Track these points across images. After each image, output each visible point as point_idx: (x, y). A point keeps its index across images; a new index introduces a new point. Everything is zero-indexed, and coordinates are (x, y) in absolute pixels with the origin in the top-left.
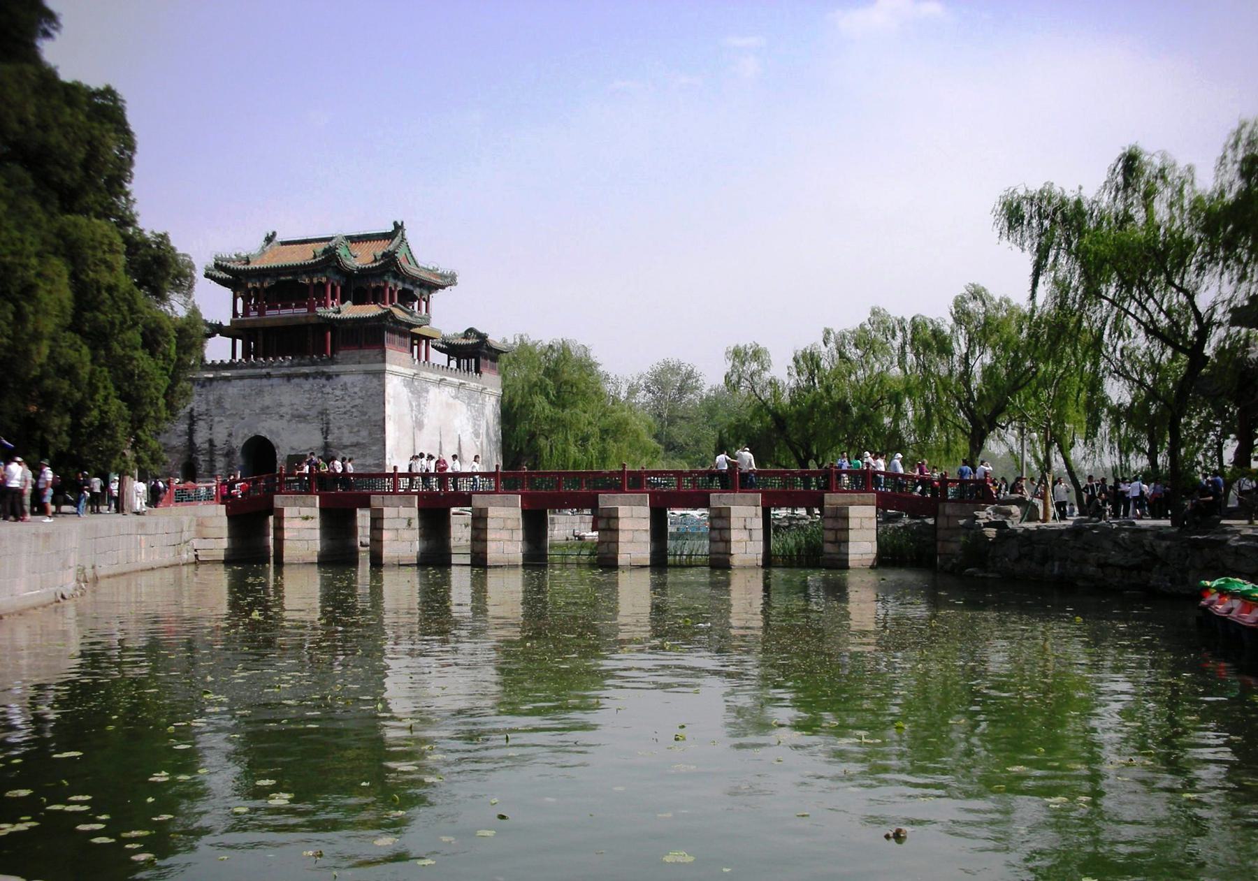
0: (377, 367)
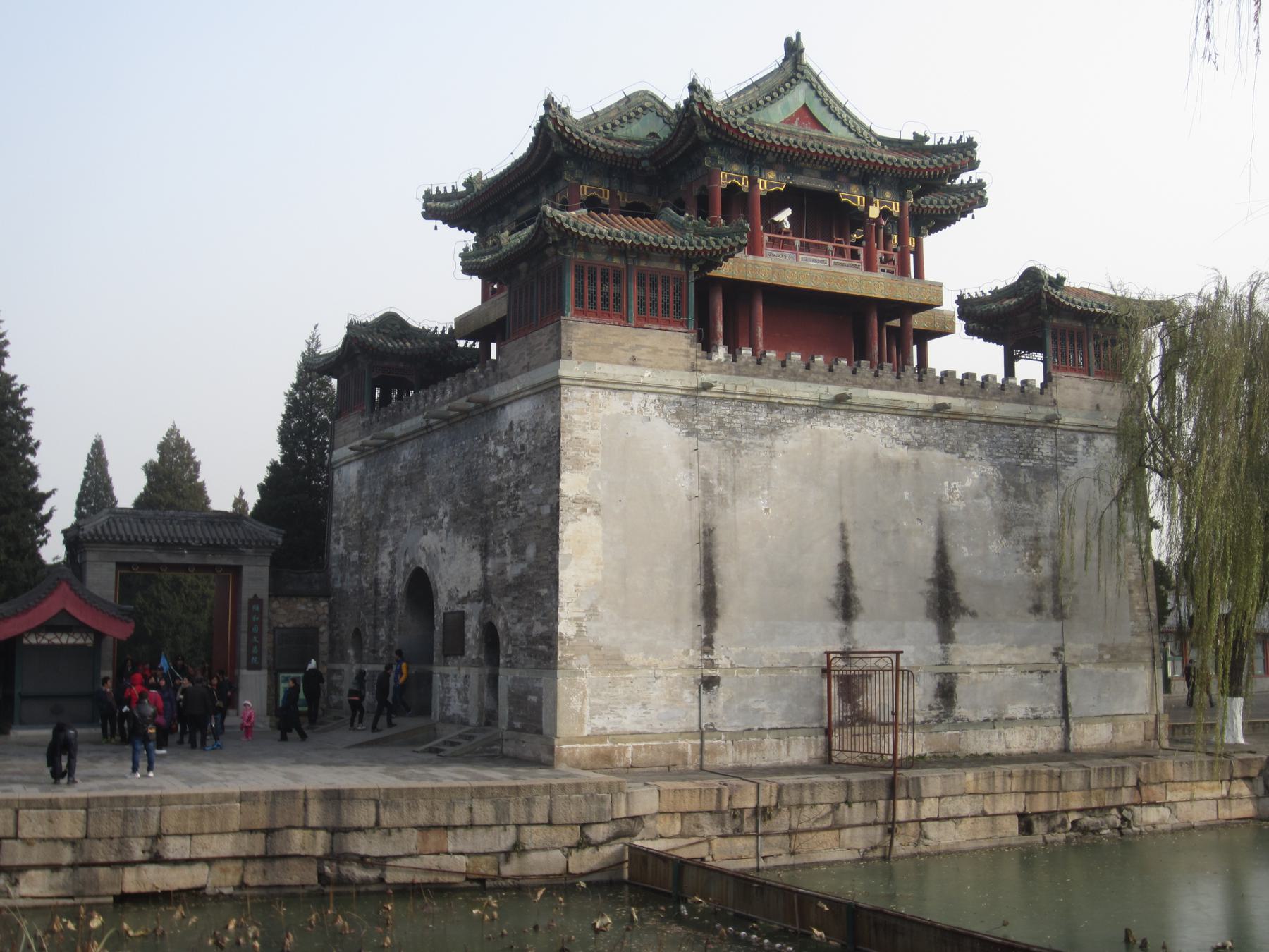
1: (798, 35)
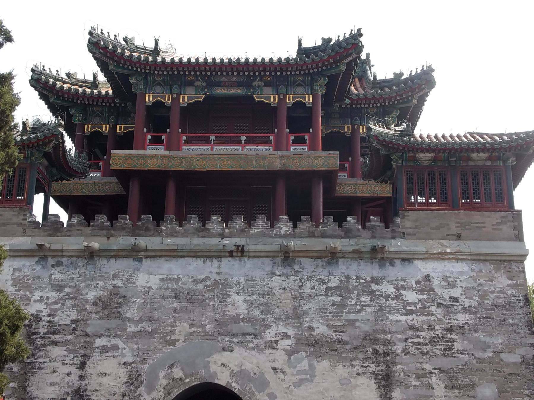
0: (506, 248)
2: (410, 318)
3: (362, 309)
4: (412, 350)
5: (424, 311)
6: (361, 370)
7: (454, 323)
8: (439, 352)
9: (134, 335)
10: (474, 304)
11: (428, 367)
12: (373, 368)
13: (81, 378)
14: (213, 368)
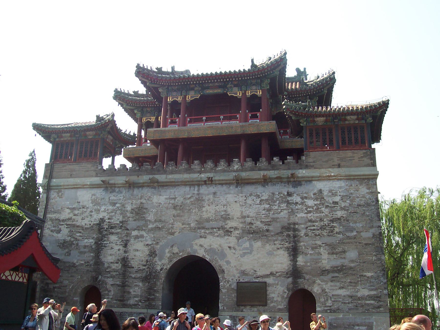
1: (305, 69)
2: (309, 215)
3: (281, 211)
4: (310, 234)
5: (318, 210)
6: (279, 246)
7: (335, 216)
8: (325, 234)
9: (152, 229)
10: (347, 205)
11: (319, 243)
12: (287, 245)
13: (125, 252)
14: (195, 247)
